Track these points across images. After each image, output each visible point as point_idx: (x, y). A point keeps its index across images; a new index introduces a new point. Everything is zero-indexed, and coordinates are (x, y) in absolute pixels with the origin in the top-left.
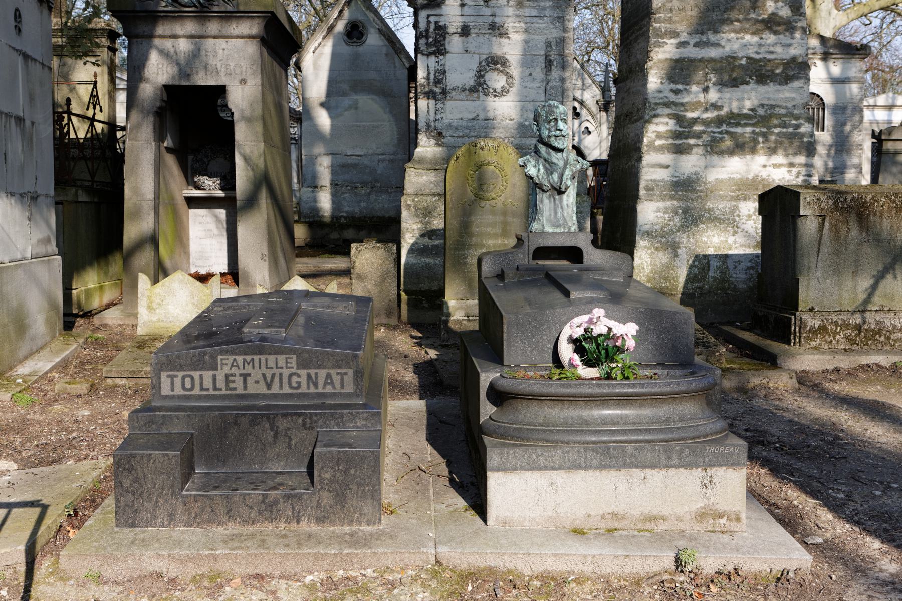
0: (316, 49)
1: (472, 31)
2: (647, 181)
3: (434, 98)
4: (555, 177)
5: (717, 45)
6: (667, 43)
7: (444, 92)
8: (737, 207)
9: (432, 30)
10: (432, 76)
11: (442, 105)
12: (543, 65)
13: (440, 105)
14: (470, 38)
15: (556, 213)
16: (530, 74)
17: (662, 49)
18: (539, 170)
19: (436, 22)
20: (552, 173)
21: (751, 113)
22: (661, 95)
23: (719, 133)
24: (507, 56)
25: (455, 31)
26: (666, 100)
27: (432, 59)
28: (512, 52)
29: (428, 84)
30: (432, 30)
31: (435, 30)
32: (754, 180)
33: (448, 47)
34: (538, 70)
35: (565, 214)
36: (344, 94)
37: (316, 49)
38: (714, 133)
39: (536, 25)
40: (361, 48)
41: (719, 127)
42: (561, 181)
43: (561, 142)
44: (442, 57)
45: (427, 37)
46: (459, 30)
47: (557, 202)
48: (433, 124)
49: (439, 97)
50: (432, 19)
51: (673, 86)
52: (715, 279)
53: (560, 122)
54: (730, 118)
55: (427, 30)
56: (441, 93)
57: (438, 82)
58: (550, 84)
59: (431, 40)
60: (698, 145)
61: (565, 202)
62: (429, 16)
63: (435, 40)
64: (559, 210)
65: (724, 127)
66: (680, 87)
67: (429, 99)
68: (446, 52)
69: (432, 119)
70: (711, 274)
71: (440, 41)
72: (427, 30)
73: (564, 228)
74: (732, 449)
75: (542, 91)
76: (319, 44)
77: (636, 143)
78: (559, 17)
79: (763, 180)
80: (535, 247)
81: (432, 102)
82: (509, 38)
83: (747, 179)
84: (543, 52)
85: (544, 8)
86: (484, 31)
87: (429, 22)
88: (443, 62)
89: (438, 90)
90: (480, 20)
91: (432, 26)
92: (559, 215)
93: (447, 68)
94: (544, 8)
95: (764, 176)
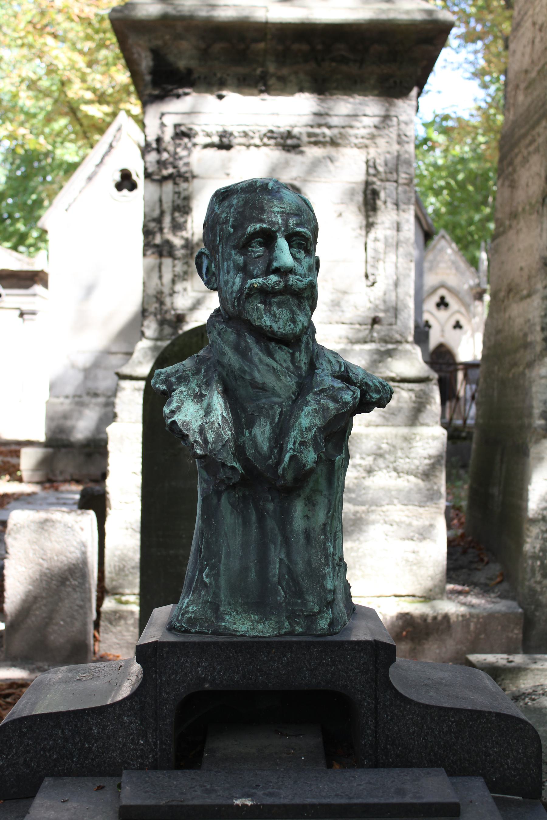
4: (262, 433)
15: (263, 561)
18: (208, 411)
19: (176, 126)
20: (250, 424)
25: (208, 140)
31: (173, 138)
35: (300, 567)
42: (282, 451)
43: (284, 313)
47: (271, 524)
53: (282, 243)
61: (298, 523)
64: (276, 555)
67: (161, 255)
72: (159, 140)
73: (292, 617)
77: (525, 335)
82: (302, 153)
87: (163, 125)
91: (169, 133)
92: (275, 570)
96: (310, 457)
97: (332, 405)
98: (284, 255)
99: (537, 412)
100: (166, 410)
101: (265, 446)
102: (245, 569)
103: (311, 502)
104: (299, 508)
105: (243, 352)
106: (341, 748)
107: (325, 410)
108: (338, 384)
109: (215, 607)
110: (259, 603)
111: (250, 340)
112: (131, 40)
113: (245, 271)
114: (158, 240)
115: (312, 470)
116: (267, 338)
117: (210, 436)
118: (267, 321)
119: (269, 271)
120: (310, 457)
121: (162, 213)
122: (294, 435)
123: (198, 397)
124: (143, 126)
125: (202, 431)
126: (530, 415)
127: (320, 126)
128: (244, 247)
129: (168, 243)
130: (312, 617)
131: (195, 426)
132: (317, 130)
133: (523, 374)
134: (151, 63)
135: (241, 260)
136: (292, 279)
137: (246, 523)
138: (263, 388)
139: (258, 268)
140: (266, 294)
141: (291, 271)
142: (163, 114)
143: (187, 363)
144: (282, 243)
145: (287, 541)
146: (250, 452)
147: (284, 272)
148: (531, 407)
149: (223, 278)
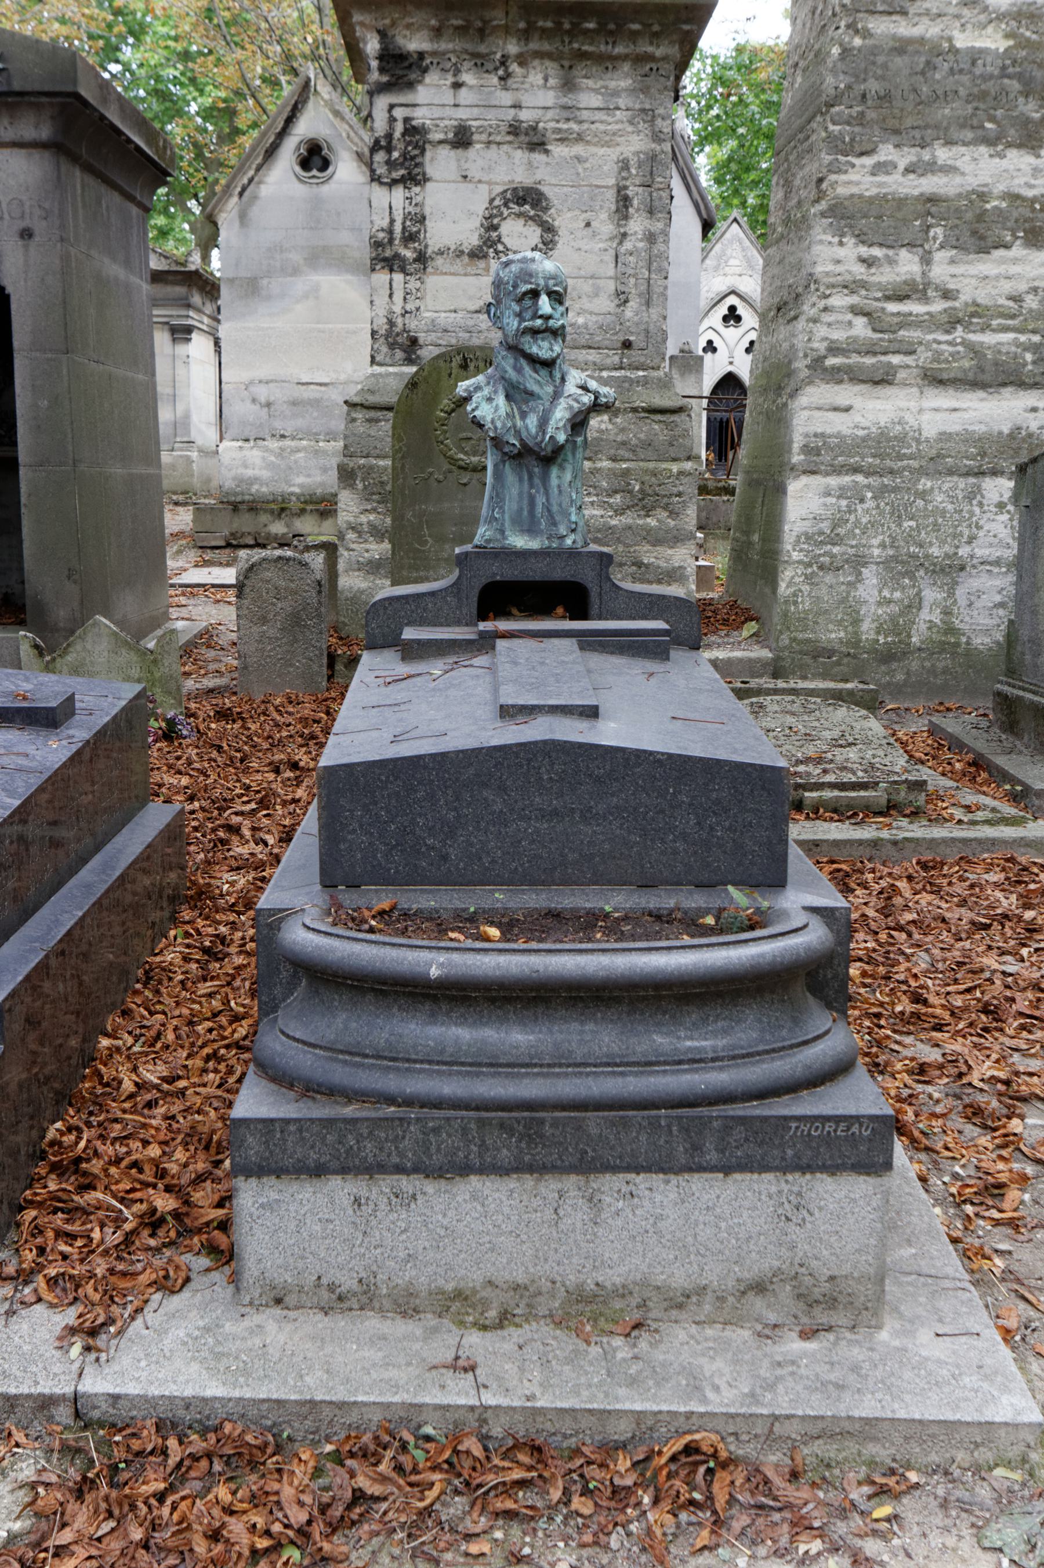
0: (244, 189)
1: (476, 137)
2: (807, 435)
3: (403, 270)
5: (949, 170)
6: (853, 166)
7: (422, 258)
8: (979, 487)
9: (397, 134)
10: (398, 228)
11: (418, 284)
12: (613, 207)
13: (413, 284)
14: (471, 153)
16: (588, 225)
17: (843, 177)
19: (407, 120)
21: (1011, 304)
22: (839, 269)
23: (949, 343)
24: (544, 189)
26: (848, 277)
27: (399, 194)
28: (553, 181)
29: (391, 241)
30: (397, 134)
31: (403, 135)
32: (1012, 436)
33: (430, 170)
34: (604, 216)
35: (555, 508)
36: (296, 272)
37: (244, 189)
38: (939, 343)
39: (602, 127)
40: (325, 189)
41: (948, 332)
42: (544, 433)
43: (545, 344)
44: (417, 189)
45: (389, 149)
46: (451, 135)
48: (399, 321)
49: (410, 268)
50: (399, 113)
51: (864, 251)
52: (931, 625)
54: (973, 315)
55: (389, 136)
56: (415, 260)
57: (410, 238)
58: (628, 245)
59: (396, 154)
60: (908, 366)
61: (554, 481)
62: (392, 107)
63: (404, 155)
65: (959, 332)
66: (877, 252)
67: (391, 270)
68: (426, 180)
69: (398, 309)
70: (925, 615)
71: (413, 158)
72: (389, 136)
74: (855, 1129)
75: (609, 257)
76: (251, 180)
77: (790, 362)
78: (643, 110)
79: (1030, 435)
80: (484, 581)
81: (398, 277)
83: (1000, 433)
84: (612, 181)
85: (616, 93)
86: (498, 139)
87: (392, 120)
88: (419, 199)
89: (409, 254)
90: (491, 114)
91: (399, 128)
92: (539, 509)
93: (427, 211)
94: (616, 93)
95: (1034, 426)
96: (562, 438)
97: (576, 405)
98: (545, 304)
99: (796, 447)
100: (469, 408)
101: (533, 431)
102: (521, 509)
103: (562, 468)
104: (554, 472)
105: (519, 370)
106: (580, 612)
107: (571, 407)
108: (580, 391)
109: (502, 532)
110: (531, 529)
111: (523, 362)
112: (357, 17)
113: (519, 315)
114: (388, 253)
115: (562, 447)
116: (534, 361)
117: (499, 425)
118: (535, 350)
119: (535, 316)
120: (562, 438)
121: (392, 221)
122: (552, 423)
123: (489, 400)
124: (368, 119)
125: (493, 421)
126: (790, 451)
127: (568, 120)
128: (520, 300)
129: (397, 256)
130: (562, 537)
131: (489, 418)
132: (561, 125)
133: (785, 405)
134: (377, 46)
135: (517, 309)
136: (551, 322)
137: (521, 480)
138: (531, 394)
139: (528, 315)
140: (535, 332)
141: (549, 317)
142: (392, 107)
143: (480, 378)
144: (544, 299)
145: (547, 493)
146: (524, 435)
147: (547, 318)
148: (791, 442)
149: (505, 321)
